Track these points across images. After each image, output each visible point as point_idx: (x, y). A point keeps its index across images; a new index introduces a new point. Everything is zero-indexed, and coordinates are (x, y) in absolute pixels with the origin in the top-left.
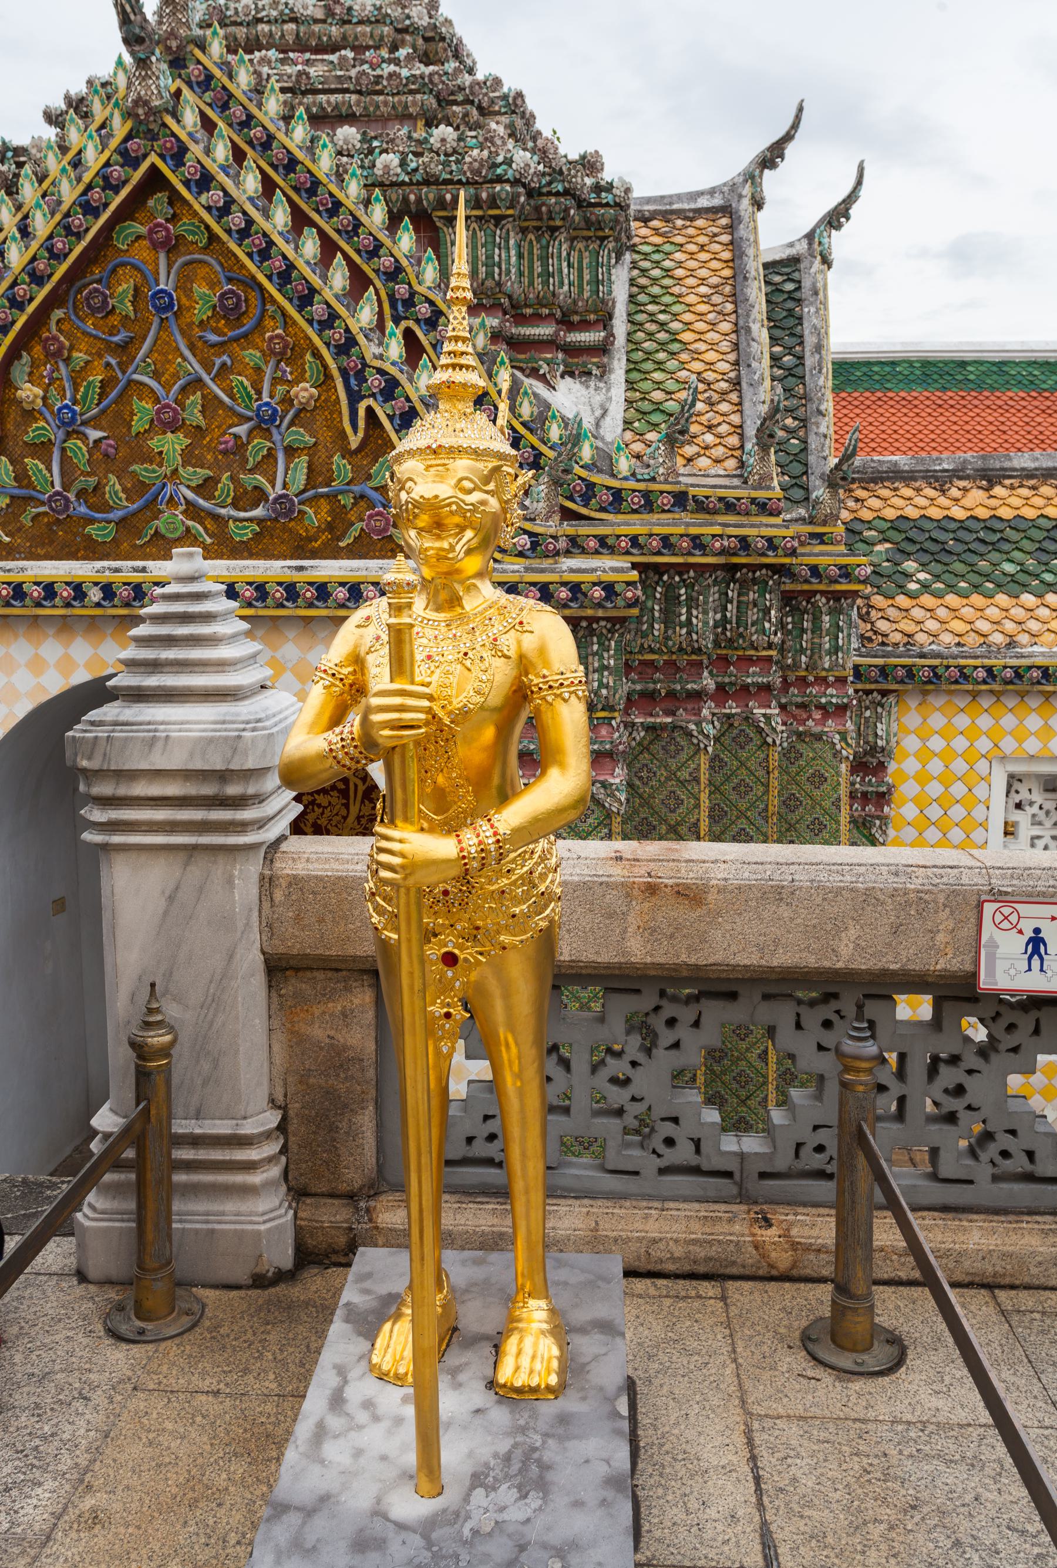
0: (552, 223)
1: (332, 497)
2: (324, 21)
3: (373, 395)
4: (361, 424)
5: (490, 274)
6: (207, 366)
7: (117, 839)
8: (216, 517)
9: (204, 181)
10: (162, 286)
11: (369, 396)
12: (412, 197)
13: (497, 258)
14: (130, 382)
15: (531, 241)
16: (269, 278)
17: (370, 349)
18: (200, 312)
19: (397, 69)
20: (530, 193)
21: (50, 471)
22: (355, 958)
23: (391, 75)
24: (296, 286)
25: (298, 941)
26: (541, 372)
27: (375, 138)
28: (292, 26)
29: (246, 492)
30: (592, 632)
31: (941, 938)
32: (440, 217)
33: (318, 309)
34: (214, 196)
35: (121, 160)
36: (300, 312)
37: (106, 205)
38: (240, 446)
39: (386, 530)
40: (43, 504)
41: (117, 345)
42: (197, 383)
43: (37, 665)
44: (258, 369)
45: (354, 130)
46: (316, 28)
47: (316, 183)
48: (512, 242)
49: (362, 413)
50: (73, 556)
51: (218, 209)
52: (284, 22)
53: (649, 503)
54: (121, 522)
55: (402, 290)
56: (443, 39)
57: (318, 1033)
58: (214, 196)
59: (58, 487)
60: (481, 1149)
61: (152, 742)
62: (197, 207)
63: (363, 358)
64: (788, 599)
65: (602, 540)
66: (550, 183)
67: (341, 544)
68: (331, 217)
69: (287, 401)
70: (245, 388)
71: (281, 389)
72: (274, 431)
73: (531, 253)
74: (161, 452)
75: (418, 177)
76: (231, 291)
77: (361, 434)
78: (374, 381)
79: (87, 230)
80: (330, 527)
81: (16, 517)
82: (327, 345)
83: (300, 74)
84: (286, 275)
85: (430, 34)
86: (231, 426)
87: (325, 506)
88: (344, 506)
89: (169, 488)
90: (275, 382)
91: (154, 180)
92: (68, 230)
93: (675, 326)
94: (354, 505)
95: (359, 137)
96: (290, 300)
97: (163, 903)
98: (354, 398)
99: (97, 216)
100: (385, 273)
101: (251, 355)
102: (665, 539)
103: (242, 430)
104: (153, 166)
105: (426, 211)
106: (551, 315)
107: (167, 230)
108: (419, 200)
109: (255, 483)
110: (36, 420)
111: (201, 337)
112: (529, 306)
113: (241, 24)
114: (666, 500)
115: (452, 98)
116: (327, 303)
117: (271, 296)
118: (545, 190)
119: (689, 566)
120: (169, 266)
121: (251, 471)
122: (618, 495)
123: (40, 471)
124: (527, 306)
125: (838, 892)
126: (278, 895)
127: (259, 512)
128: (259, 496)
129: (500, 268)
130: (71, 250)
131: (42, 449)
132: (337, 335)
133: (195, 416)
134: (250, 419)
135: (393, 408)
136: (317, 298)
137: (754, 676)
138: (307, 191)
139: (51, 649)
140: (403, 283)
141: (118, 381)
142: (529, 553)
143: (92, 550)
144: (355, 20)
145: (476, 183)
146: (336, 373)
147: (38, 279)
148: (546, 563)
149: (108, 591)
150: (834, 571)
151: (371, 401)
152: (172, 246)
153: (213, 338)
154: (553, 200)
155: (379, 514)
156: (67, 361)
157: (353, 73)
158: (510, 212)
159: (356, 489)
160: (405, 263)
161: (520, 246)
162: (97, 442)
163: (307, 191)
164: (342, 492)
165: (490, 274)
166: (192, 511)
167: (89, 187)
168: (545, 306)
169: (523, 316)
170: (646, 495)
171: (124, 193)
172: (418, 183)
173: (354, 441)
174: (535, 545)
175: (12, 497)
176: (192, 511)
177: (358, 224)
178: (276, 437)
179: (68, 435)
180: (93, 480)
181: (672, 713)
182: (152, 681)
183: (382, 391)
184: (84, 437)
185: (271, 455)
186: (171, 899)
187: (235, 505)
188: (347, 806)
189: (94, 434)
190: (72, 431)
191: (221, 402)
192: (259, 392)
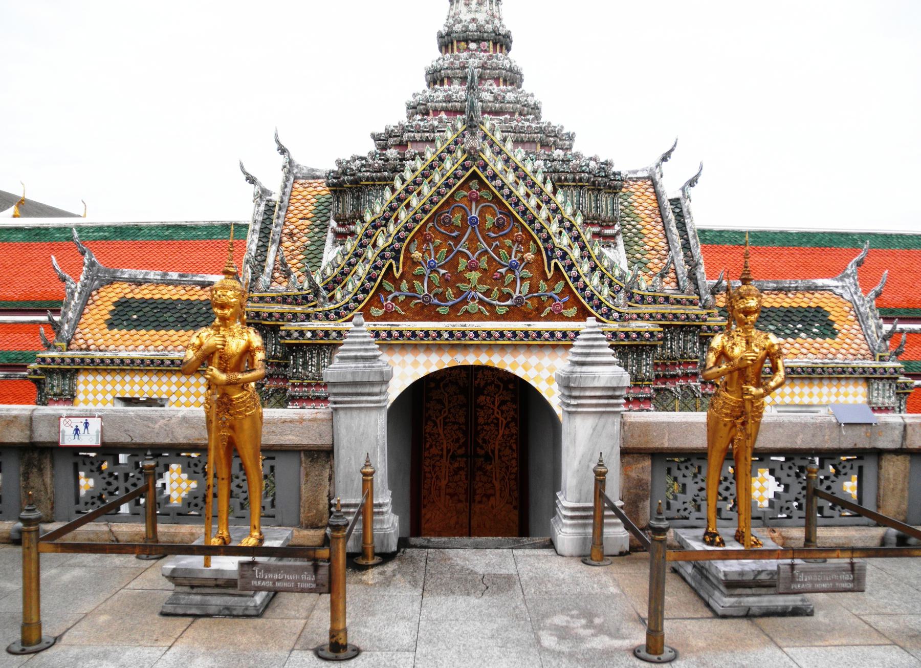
1: (539, 297)
4: (552, 269)
6: (490, 246)
7: (580, 410)
9: (494, 177)
14: (459, 252)
17: (556, 240)
18: (488, 225)
21: (423, 285)
22: (649, 449)
24: (529, 216)
25: (634, 443)
30: (643, 350)
31: (827, 437)
33: (537, 225)
37: (454, 185)
38: (502, 277)
42: (486, 252)
43: (415, 364)
44: (510, 248)
46: (490, 104)
47: (526, 175)
49: (552, 265)
50: (431, 320)
53: (655, 301)
54: (452, 307)
57: (633, 474)
59: (426, 292)
60: (683, 513)
61: (595, 378)
64: (701, 338)
65: (638, 315)
69: (522, 259)
71: (519, 255)
78: (558, 253)
80: (537, 309)
81: (408, 304)
84: (524, 213)
87: (535, 301)
89: (471, 294)
90: (517, 252)
91: (474, 175)
92: (439, 193)
93: (639, 226)
97: (591, 431)
98: (550, 259)
99: (450, 189)
101: (508, 242)
102: (663, 315)
103: (503, 270)
114: (662, 299)
119: (671, 325)
120: (477, 207)
122: (643, 297)
125: (796, 424)
126: (626, 428)
127: (509, 303)
128: (509, 296)
131: (421, 277)
132: (544, 235)
133: (484, 264)
134: (505, 266)
137: (690, 369)
139: (422, 357)
143: (439, 318)
146: (543, 250)
147: (425, 211)
148: (625, 324)
149: (451, 334)
150: (716, 328)
152: (478, 200)
153: (493, 235)
156: (433, 243)
160: (560, 206)
162: (444, 274)
166: (481, 302)
170: (654, 297)
171: (462, 180)
174: (620, 317)
175: (406, 296)
176: (481, 302)
177: (542, 191)
178: (517, 273)
179: (431, 272)
180: (441, 290)
181: (665, 384)
182: (589, 359)
184: (438, 273)
185: (514, 281)
186: (594, 430)
187: (499, 300)
188: (498, 430)
189: (442, 271)
190: (433, 270)
191: (495, 260)
192: (510, 256)
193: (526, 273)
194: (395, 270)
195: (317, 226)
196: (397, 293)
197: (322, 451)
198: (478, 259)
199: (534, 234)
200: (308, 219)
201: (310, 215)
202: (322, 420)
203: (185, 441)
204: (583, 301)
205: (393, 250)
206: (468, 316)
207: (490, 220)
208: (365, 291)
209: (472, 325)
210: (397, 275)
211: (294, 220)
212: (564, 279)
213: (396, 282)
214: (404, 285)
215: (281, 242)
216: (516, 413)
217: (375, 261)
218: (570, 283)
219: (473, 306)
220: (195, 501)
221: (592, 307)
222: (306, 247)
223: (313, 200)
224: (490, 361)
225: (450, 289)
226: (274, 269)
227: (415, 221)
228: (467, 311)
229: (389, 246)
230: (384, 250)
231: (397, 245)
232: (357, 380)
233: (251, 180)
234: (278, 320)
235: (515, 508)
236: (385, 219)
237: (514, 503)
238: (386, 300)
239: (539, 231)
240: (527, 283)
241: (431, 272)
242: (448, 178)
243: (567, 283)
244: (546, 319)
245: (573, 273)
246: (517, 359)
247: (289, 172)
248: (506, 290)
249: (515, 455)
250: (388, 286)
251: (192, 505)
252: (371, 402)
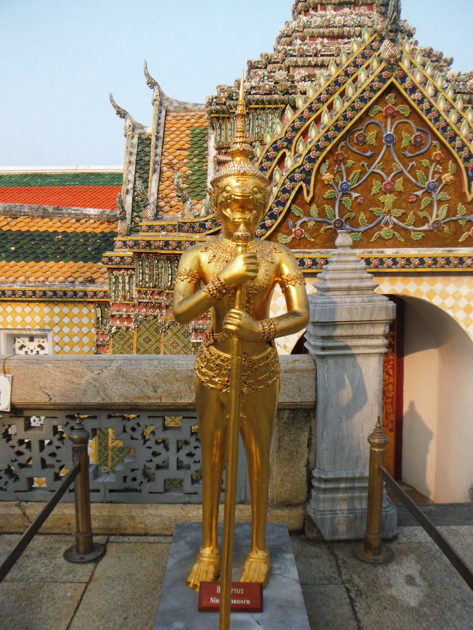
1: (456, 221)
6: (405, 166)
8: (406, 230)
9: (413, 89)
10: (389, 132)
16: (438, 129)
18: (405, 143)
21: (334, 209)
33: (458, 143)
34: (417, 95)
36: (450, 143)
37: (370, 98)
40: (330, 224)
41: (367, 157)
42: (401, 173)
44: (427, 168)
51: (418, 101)
58: (417, 95)
59: (337, 217)
62: (410, 100)
70: (422, 176)
71: (437, 176)
72: (433, 193)
74: (384, 203)
76: (419, 135)
82: (460, 157)
86: (414, 192)
90: (435, 172)
91: (392, 87)
92: (353, 108)
96: (446, 139)
99: (366, 103)
101: (425, 162)
103: (419, 193)
104: (392, 83)
107: (394, 109)
109: (424, 215)
111: (403, 154)
116: (461, 140)
127: (425, 227)
128: (425, 220)
134: (423, 188)
136: (457, 138)
141: (367, 172)
146: (463, 169)
153: (409, 155)
156: (345, 164)
162: (356, 198)
164: (461, 219)
166: (396, 227)
175: (316, 221)
180: (354, 214)
184: (350, 196)
187: (414, 225)
189: (355, 195)
192: (427, 178)
193: (444, 196)
194: (305, 192)
195: (195, 156)
196: (305, 219)
197: (299, 410)
198: (393, 180)
199: (454, 152)
200: (185, 150)
201: (187, 146)
202: (302, 371)
203: (121, 401)
206: (383, 242)
207: (407, 139)
209: (389, 252)
210: (308, 199)
211: (172, 150)
213: (306, 206)
214: (314, 210)
215: (161, 172)
216: (393, 340)
217: (284, 184)
219: (385, 232)
220: (132, 475)
222: (187, 177)
223: (188, 132)
224: (418, 290)
225: (362, 214)
226: (158, 198)
227: (327, 139)
228: (380, 237)
229: (299, 167)
230: (293, 171)
231: (308, 166)
232: (356, 318)
233: (122, 114)
234: (175, 249)
235: (391, 430)
236: (287, 140)
237: (390, 426)
238: (295, 226)
239: (460, 149)
240: (445, 208)
241: (343, 195)
242: (364, 91)
244: (464, 244)
246: (433, 288)
247: (161, 104)
248: (422, 214)
249: (391, 380)
250: (296, 210)
251: (129, 479)
252: (370, 347)
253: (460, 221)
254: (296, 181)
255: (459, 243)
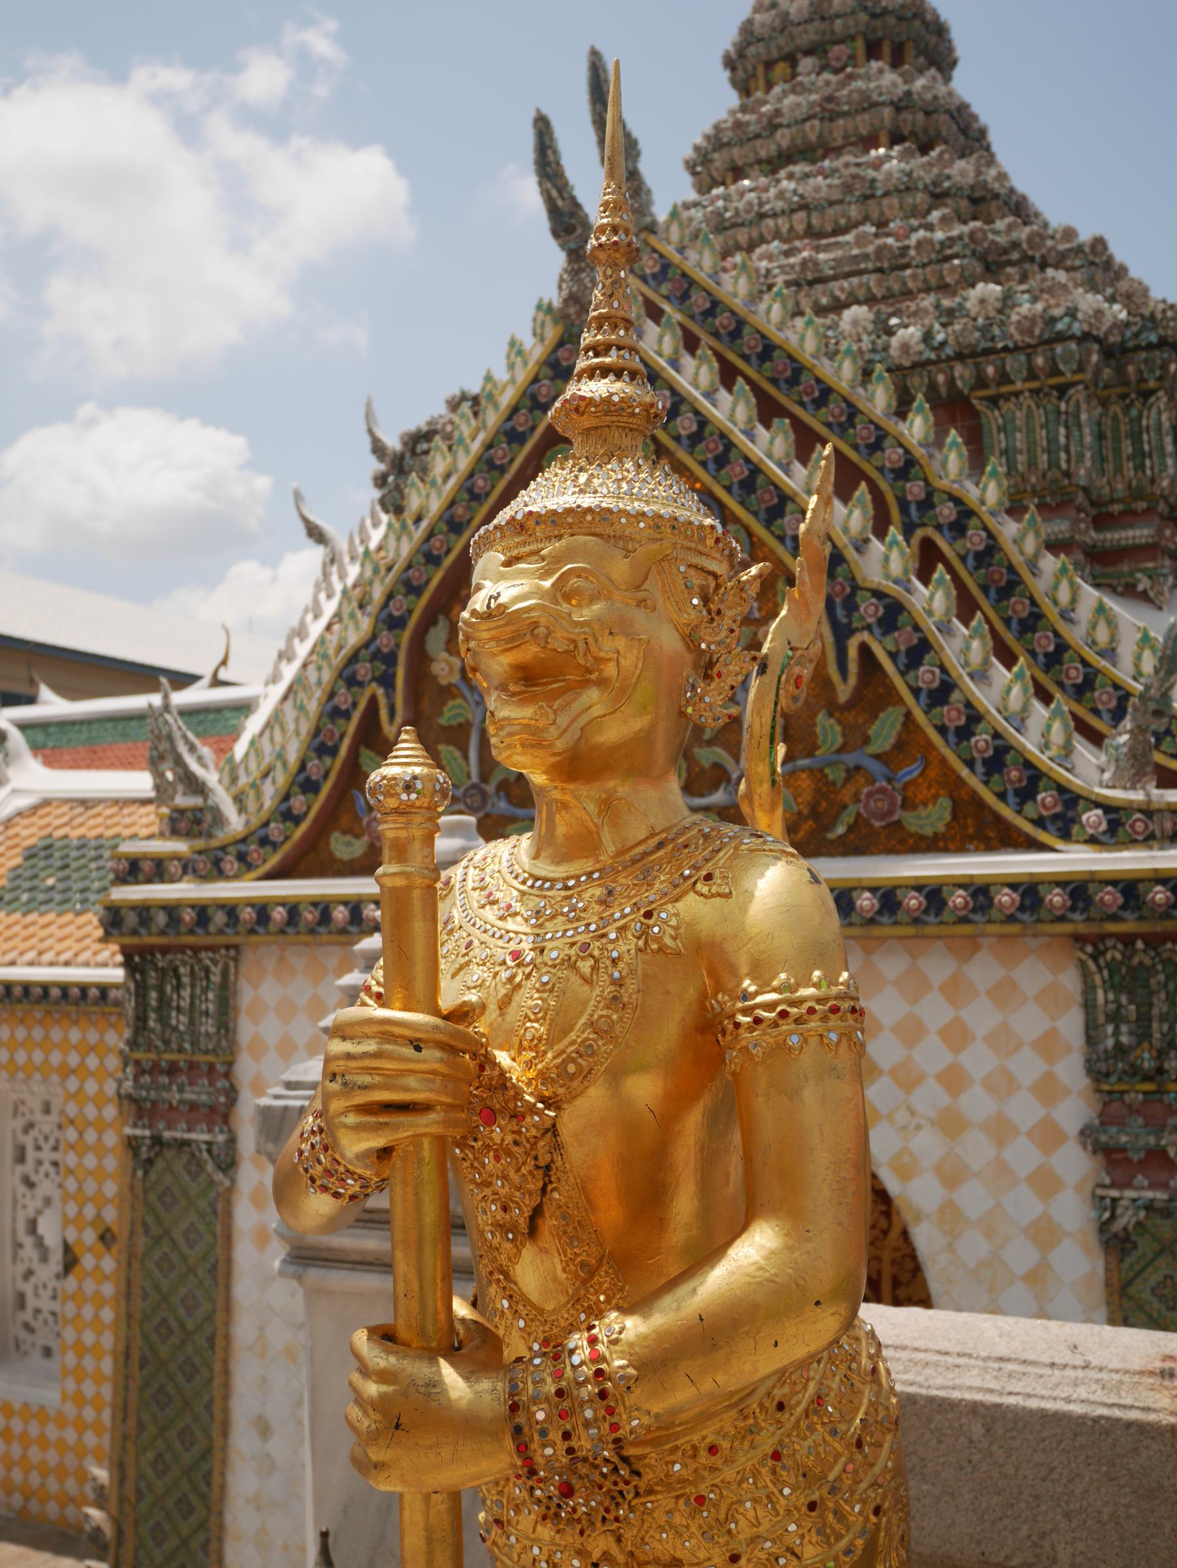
0: (1143, 386)
2: (840, 202)
3: (869, 628)
4: (853, 667)
5: (1053, 463)
11: (863, 628)
12: (941, 378)
13: (1062, 440)
15: (1115, 417)
16: (728, 489)
19: (928, 234)
20: (1109, 353)
21: (466, 757)
23: (920, 244)
26: (1140, 588)
27: (894, 314)
28: (802, 215)
29: (702, 770)
32: (980, 399)
35: (550, 372)
37: (533, 428)
39: (890, 813)
45: (865, 308)
46: (831, 212)
48: (1084, 417)
52: (793, 211)
55: (915, 490)
56: (996, 196)
59: (475, 778)
63: (853, 579)
66: (1137, 335)
67: (831, 836)
68: (818, 408)
73: (1116, 429)
75: (949, 351)
77: (852, 680)
78: (869, 609)
79: (512, 461)
80: (815, 813)
83: (804, 262)
85: (977, 194)
88: (834, 783)
94: (847, 780)
95: (871, 316)
96: (755, 514)
100: (892, 470)
105: (960, 392)
106: (1150, 511)
108: (951, 382)
110: (454, 697)
112: (1118, 501)
113: (742, 225)
115: (1004, 258)
117: (733, 513)
118: (1130, 344)
121: (710, 743)
123: (455, 759)
124: (1113, 501)
129: (1068, 452)
130: (493, 487)
135: (896, 642)
138: (787, 381)
140: (916, 479)
142: (1104, 839)
144: (879, 192)
145: (1029, 346)
151: (865, 636)
154: (1143, 355)
155: (882, 791)
157: (870, 249)
158: (1078, 377)
159: (851, 759)
160: (919, 452)
161: (1099, 424)
163: (787, 381)
165: (1053, 463)
167: (514, 410)
168: (1140, 497)
169: (1110, 516)
172: (949, 359)
173: (844, 692)
174: (1114, 826)
177: (853, 412)
183: (880, 622)
204: (964, 772)
205: (376, 656)
208: (310, 787)
212: (900, 701)
218: (919, 715)
221: (1002, 796)
231: (385, 640)
243: (908, 715)
245: (926, 675)
253: (827, 771)
254: (361, 684)
255: (831, 842)
